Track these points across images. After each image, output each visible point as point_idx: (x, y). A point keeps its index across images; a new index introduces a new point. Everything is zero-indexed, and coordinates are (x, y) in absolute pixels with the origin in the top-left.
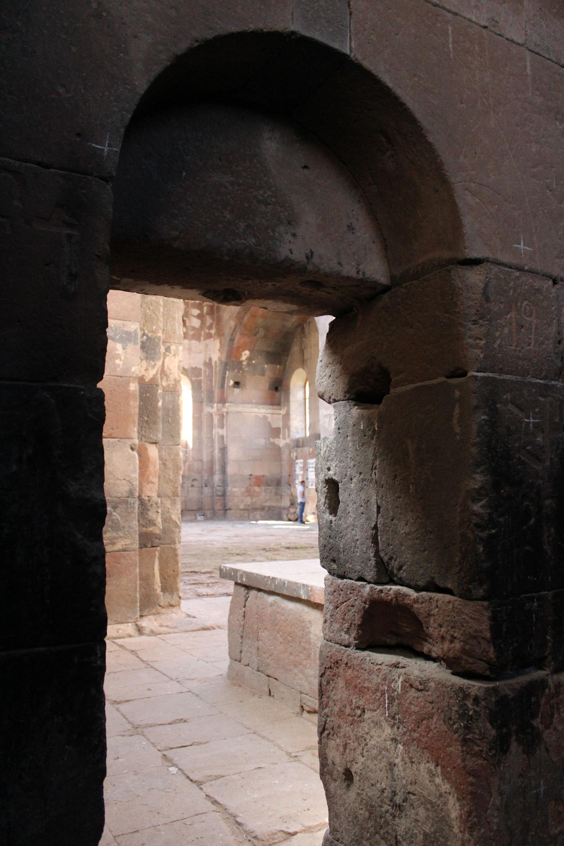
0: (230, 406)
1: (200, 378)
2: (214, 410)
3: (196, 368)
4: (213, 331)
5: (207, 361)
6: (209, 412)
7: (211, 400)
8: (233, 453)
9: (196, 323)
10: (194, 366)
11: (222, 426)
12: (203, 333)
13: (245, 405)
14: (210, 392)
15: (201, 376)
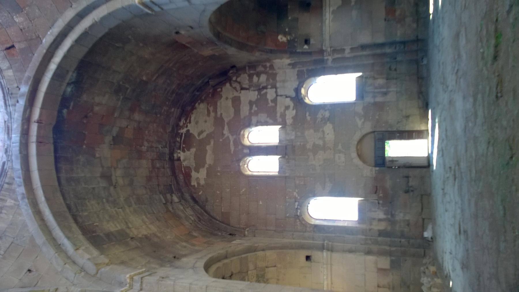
0: (325, 46)
1: (305, 71)
2: (330, 58)
3: (298, 75)
4: (268, 64)
5: (291, 67)
6: (332, 62)
7: (322, 61)
8: (365, 38)
9: (263, 78)
10: (296, 77)
11: (343, 50)
12: (270, 72)
13: (324, 33)
14: (316, 62)
15: (303, 70)
